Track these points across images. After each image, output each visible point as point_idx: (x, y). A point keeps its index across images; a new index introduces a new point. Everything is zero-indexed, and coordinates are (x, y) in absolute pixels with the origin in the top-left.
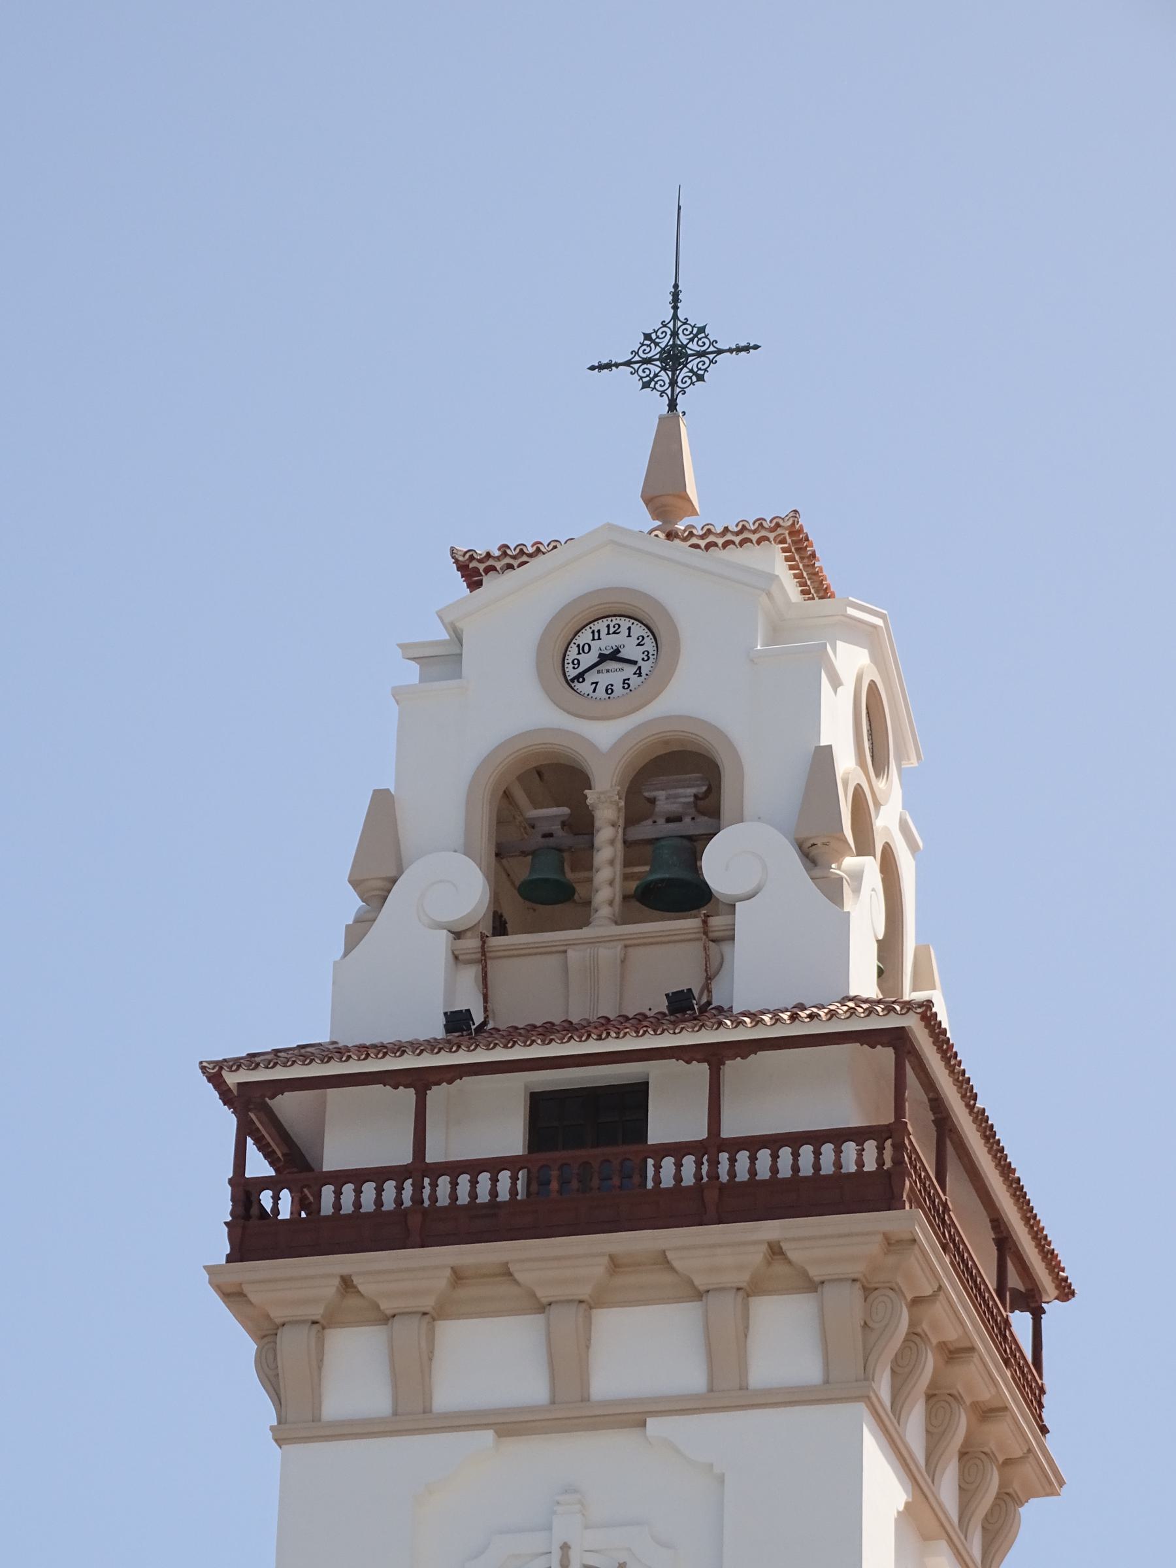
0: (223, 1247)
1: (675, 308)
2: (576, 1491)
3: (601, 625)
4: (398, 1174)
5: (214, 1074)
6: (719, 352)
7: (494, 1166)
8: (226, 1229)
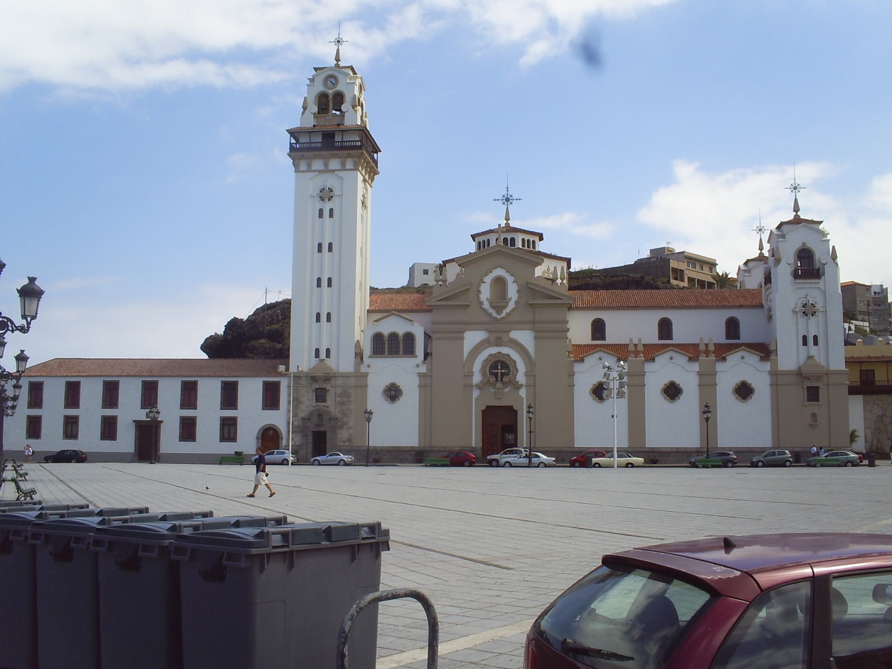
4: (307, 143)
5: (287, 131)
7: (318, 143)
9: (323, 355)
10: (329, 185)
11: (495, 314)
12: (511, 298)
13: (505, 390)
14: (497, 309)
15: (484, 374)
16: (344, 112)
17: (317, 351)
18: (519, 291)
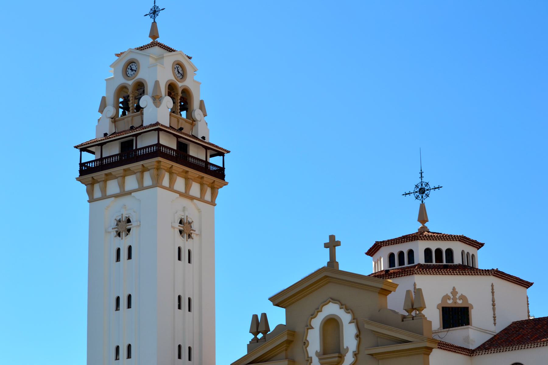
0: (78, 174)
1: (155, 4)
3: (131, 65)
6: (160, 10)
7: (115, 156)
8: (79, 171)
12: (347, 347)
16: (143, 108)
18: (357, 336)
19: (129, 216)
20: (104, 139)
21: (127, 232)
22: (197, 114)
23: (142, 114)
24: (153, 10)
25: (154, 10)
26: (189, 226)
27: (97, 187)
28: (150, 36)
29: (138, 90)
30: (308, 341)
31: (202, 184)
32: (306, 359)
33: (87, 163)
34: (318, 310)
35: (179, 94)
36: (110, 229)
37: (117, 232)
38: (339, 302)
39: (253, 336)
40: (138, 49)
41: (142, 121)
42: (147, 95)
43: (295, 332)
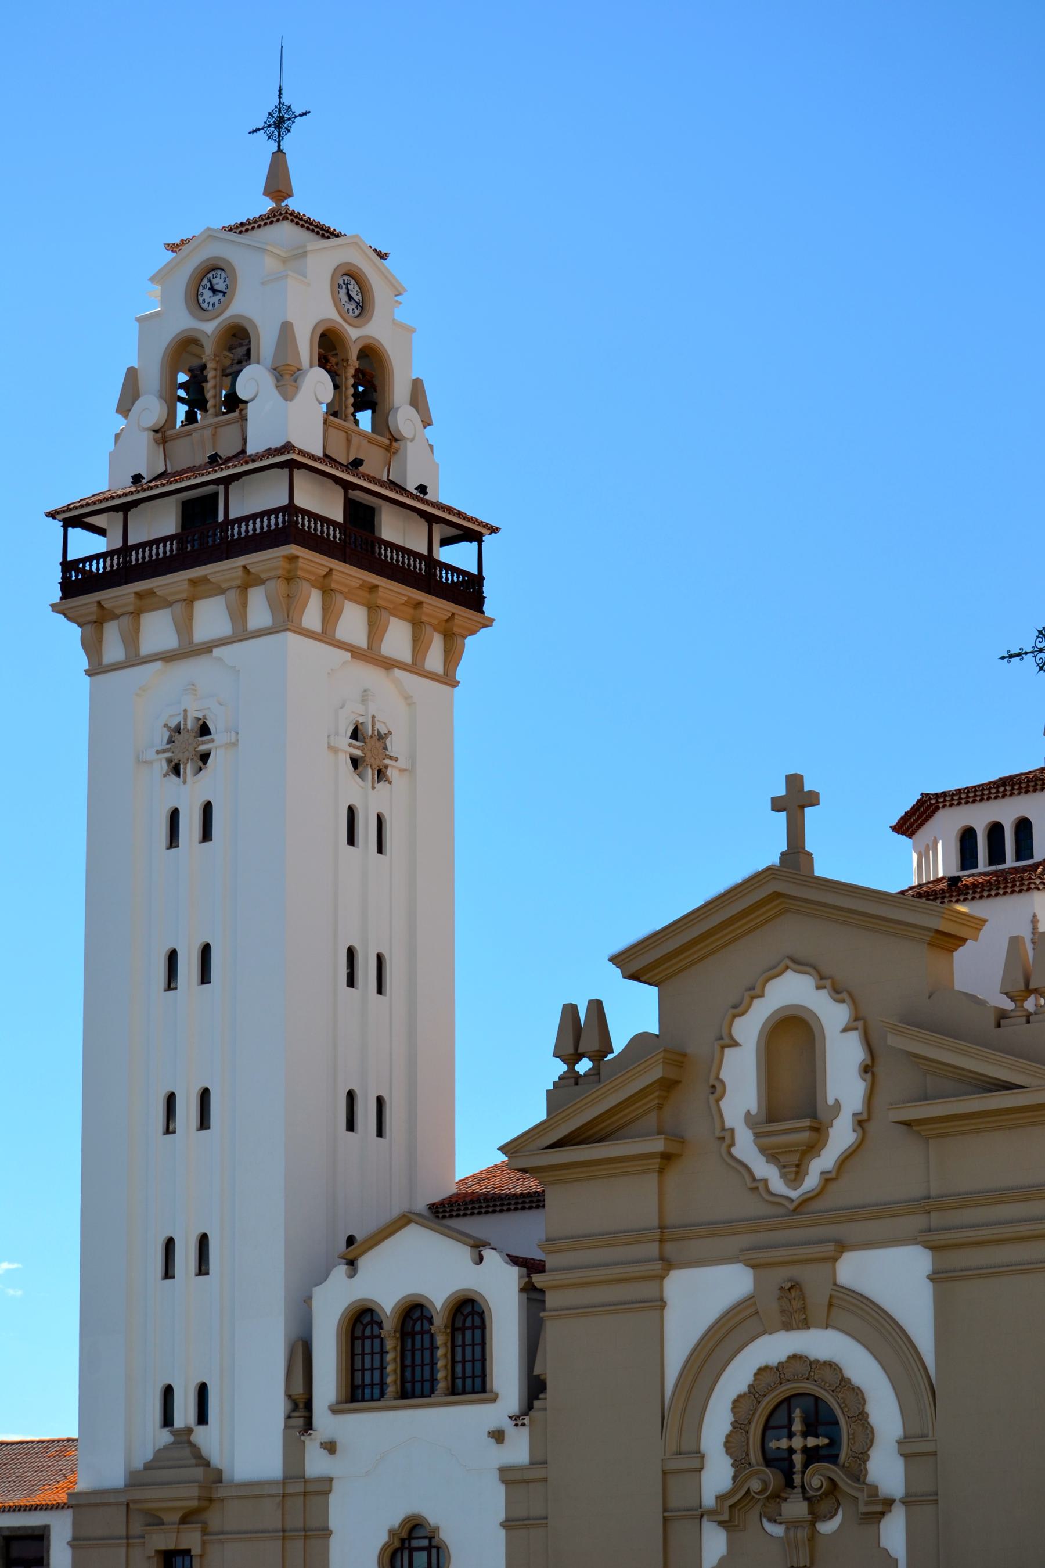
0: (56, 594)
2: (193, 685)
3: (210, 275)
7: (164, 540)
8: (59, 585)
9: (184, 1412)
10: (195, 711)
11: (778, 1185)
13: (828, 1527)
14: (783, 1159)
15: (740, 1465)
16: (246, 402)
17: (168, 1392)
18: (867, 1069)
19: (204, 717)
20: (132, 493)
21: (200, 764)
22: (404, 419)
23: (244, 419)
24: (276, 115)
25: (279, 117)
26: (378, 744)
27: (112, 632)
28: (266, 193)
29: (231, 349)
30: (722, 1082)
31: (417, 625)
32: (718, 1134)
33: (84, 560)
34: (752, 993)
35: (350, 362)
36: (151, 755)
37: (169, 761)
38: (815, 968)
39: (564, 1068)
40: (231, 230)
41: (245, 440)
42: (258, 363)
43: (685, 1055)
